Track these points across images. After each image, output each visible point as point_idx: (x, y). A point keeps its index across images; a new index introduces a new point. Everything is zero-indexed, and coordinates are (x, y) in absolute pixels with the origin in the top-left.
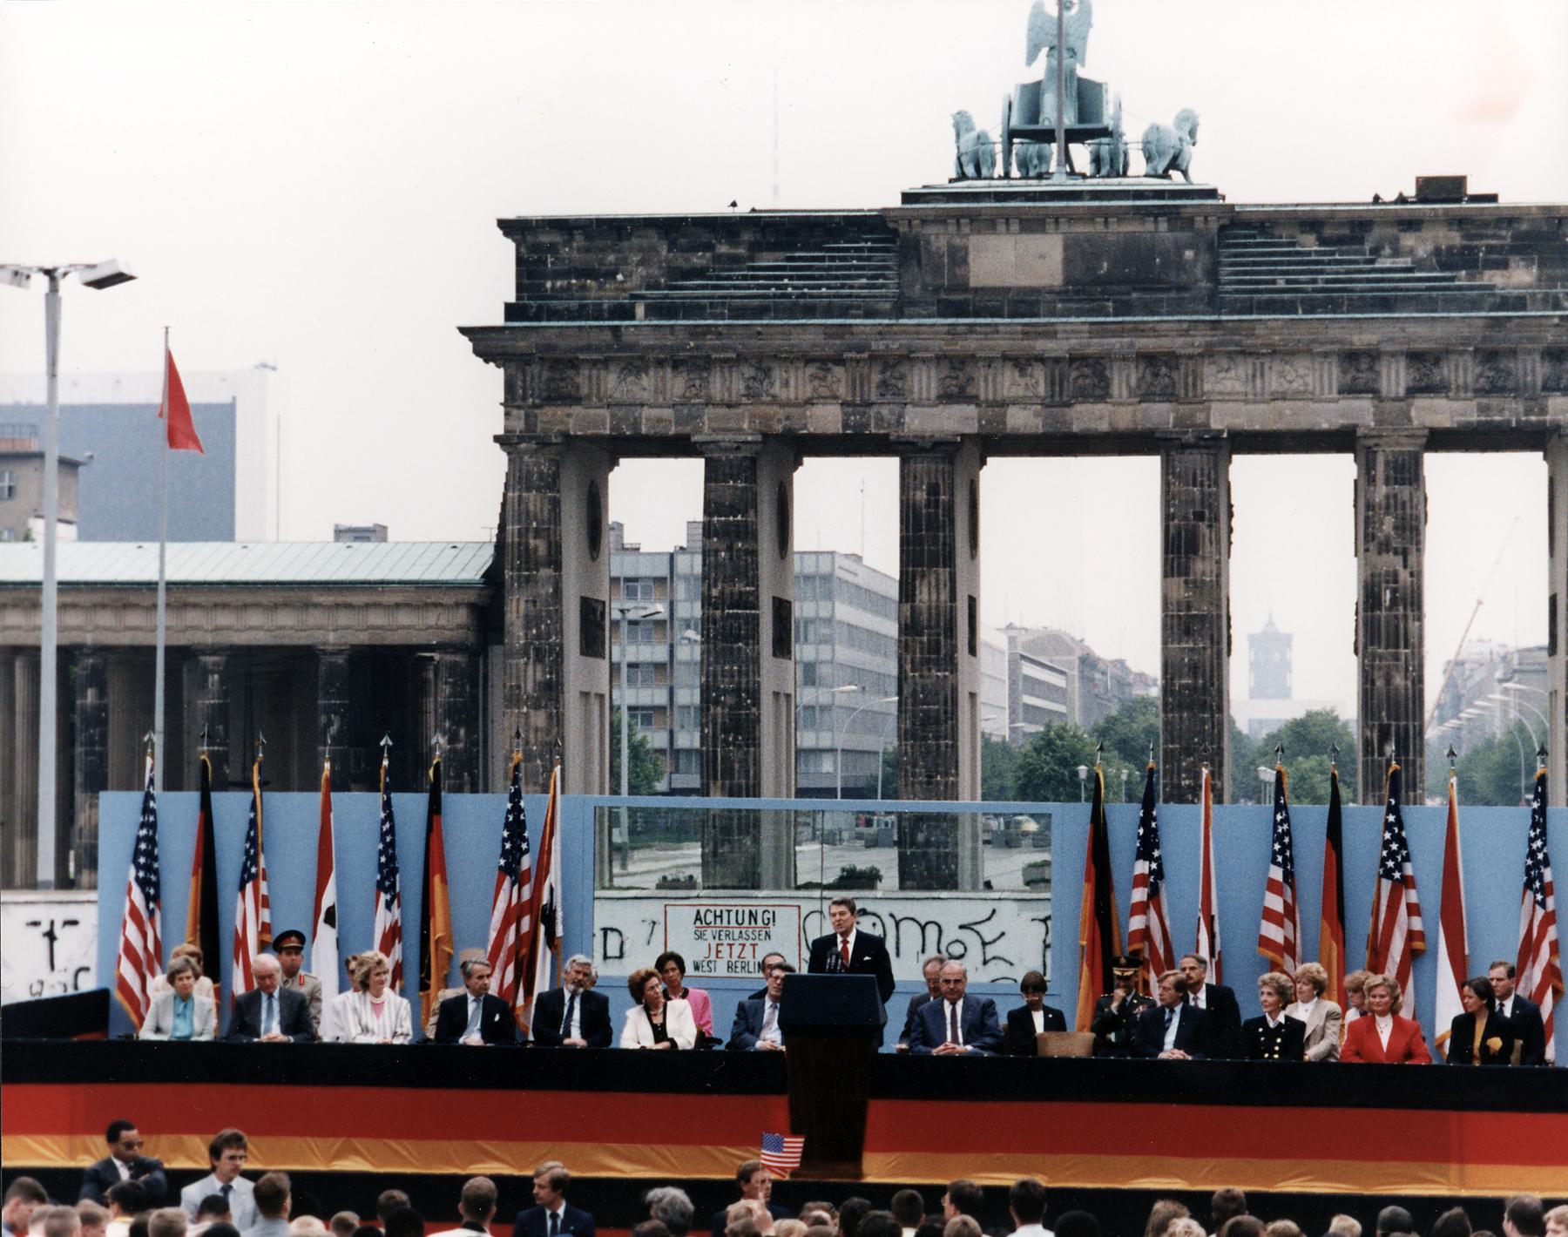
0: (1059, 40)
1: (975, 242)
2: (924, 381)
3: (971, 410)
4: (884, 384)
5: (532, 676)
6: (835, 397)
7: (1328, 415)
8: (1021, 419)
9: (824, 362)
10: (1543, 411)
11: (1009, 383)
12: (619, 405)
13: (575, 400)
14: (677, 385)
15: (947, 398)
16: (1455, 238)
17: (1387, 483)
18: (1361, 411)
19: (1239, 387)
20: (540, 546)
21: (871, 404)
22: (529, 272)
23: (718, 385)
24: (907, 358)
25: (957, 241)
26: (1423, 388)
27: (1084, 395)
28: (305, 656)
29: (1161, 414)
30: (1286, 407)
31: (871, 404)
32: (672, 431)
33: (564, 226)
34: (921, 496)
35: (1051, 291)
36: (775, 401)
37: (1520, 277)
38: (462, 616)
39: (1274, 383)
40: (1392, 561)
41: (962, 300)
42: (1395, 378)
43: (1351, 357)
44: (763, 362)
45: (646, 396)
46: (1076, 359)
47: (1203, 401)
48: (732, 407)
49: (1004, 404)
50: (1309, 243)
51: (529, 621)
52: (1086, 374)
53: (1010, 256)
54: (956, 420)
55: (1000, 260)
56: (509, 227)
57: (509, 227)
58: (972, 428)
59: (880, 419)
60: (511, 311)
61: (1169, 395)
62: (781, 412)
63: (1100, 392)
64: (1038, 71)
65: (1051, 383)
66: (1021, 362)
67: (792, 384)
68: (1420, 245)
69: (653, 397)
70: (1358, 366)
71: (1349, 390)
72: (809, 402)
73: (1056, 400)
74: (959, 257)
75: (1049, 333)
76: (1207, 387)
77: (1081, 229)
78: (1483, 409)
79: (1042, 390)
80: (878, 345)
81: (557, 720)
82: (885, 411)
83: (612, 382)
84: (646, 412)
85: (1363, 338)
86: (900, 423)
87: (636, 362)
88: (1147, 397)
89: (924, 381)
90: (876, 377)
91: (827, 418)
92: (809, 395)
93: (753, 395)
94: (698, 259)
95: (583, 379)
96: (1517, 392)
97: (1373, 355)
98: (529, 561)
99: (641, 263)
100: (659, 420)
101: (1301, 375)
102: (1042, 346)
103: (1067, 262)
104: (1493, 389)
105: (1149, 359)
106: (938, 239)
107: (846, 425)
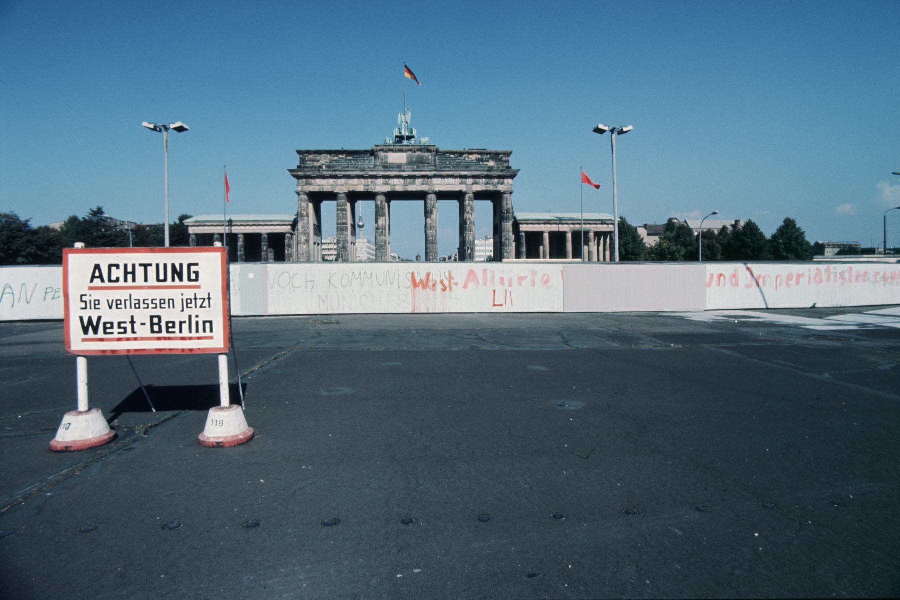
5: (303, 238)
7: (457, 188)
8: (399, 189)
11: (396, 181)
13: (311, 185)
14: (331, 181)
18: (463, 188)
20: (305, 213)
22: (303, 161)
28: (259, 236)
29: (425, 188)
33: (309, 152)
34: (379, 203)
37: (492, 164)
38: (290, 227)
41: (386, 167)
43: (461, 177)
46: (410, 177)
50: (452, 156)
51: (303, 228)
54: (387, 189)
56: (299, 152)
57: (299, 152)
60: (299, 167)
63: (414, 184)
68: (474, 157)
71: (462, 183)
73: (405, 185)
74: (386, 158)
81: (308, 247)
83: (318, 181)
87: (324, 177)
94: (336, 158)
96: (492, 184)
98: (303, 216)
101: (451, 180)
102: (402, 174)
103: (408, 158)
104: (488, 184)
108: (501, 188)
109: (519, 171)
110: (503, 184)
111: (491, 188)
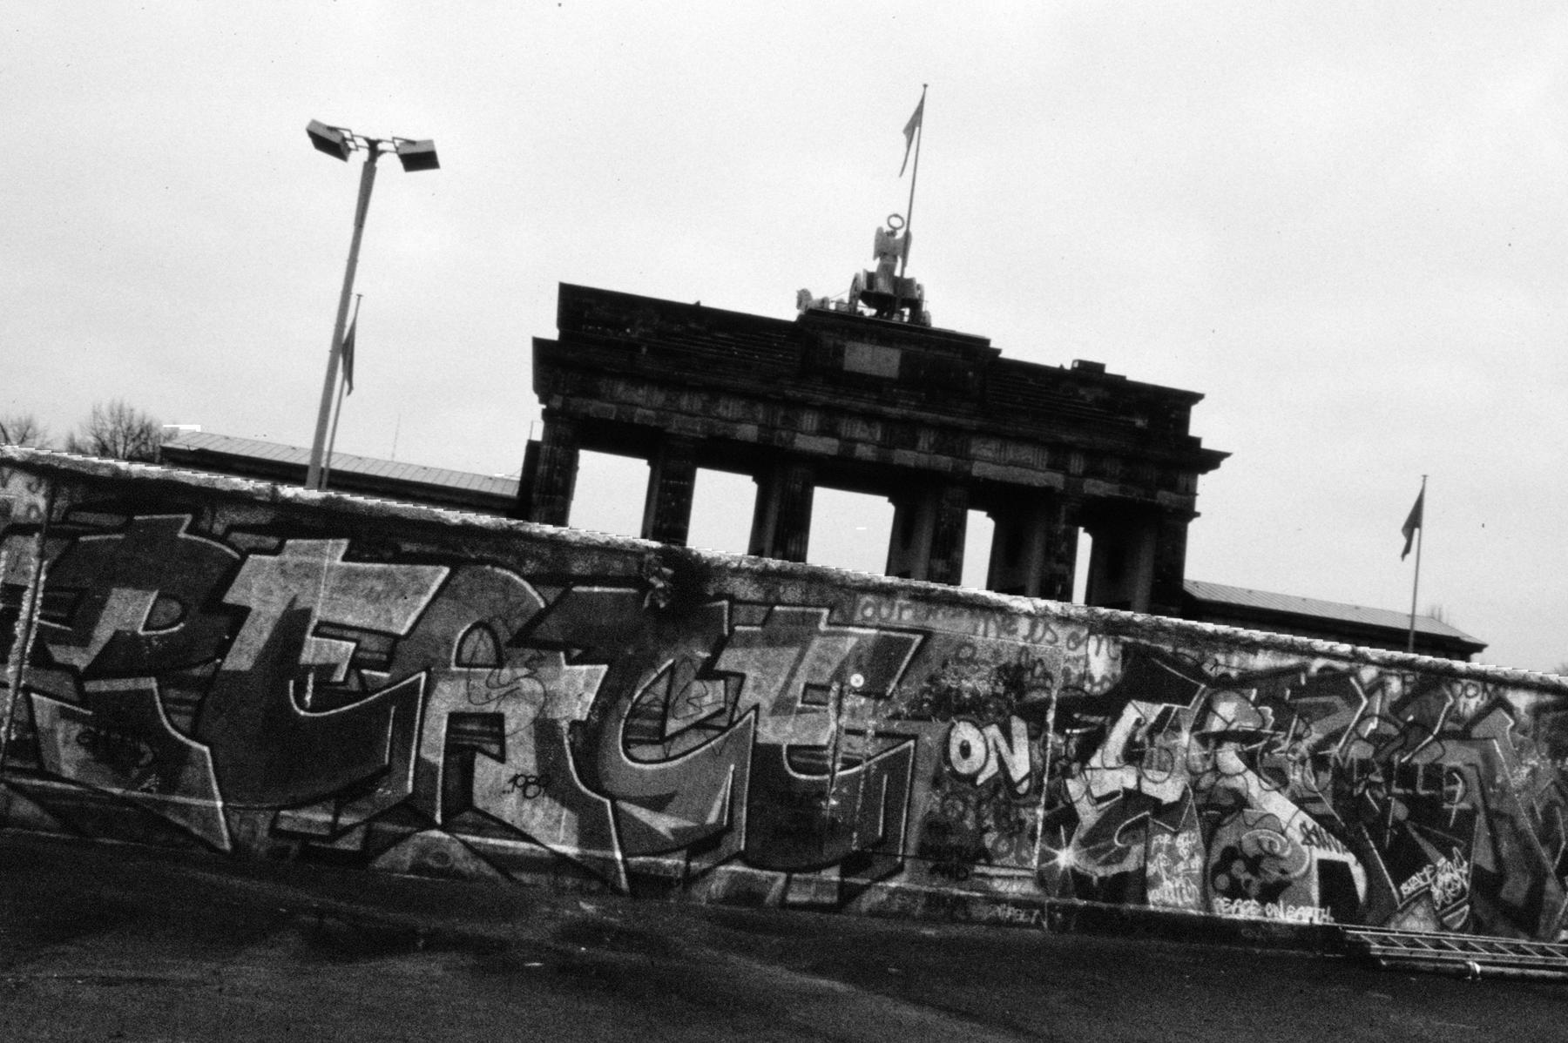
0: (891, 247)
1: (849, 345)
2: (810, 421)
3: (836, 442)
4: (785, 418)
6: (753, 420)
8: (864, 451)
9: (750, 397)
10: (1154, 497)
11: (859, 430)
12: (624, 403)
13: (596, 395)
14: (659, 398)
15: (822, 432)
16: (1107, 395)
17: (1066, 522)
18: (1057, 480)
19: (990, 454)
21: (774, 428)
23: (684, 402)
24: (804, 405)
25: (839, 342)
26: (1091, 472)
27: (904, 446)
29: (944, 462)
30: (1017, 471)
31: (774, 428)
32: (654, 424)
35: (889, 379)
36: (719, 417)
39: (1011, 455)
40: (1060, 568)
42: (1077, 465)
44: (716, 392)
45: (639, 400)
46: (905, 421)
47: (971, 459)
48: (688, 415)
49: (856, 441)
52: (904, 432)
53: (867, 356)
54: (826, 446)
55: (866, 358)
58: (833, 451)
59: (781, 439)
61: (950, 452)
62: (721, 424)
63: (913, 446)
64: (873, 265)
65: (884, 435)
66: (869, 418)
67: (729, 409)
69: (645, 403)
70: (1058, 456)
71: (1052, 467)
72: (739, 421)
73: (886, 445)
74: (839, 352)
75: (894, 405)
76: (973, 451)
77: (912, 348)
78: (1121, 490)
79: (878, 436)
80: (790, 393)
82: (784, 434)
84: (639, 411)
85: (1065, 437)
86: (792, 441)
88: (938, 452)
89: (810, 421)
90: (782, 413)
91: (749, 432)
92: (740, 415)
93: (706, 411)
95: (603, 385)
97: (1070, 448)
99: (644, 325)
100: (646, 417)
101: (1026, 453)
105: (942, 429)
106: (829, 340)
107: (759, 437)
108: (1165, 497)
109: (1227, 455)
110: (1172, 486)
111: (1136, 493)
